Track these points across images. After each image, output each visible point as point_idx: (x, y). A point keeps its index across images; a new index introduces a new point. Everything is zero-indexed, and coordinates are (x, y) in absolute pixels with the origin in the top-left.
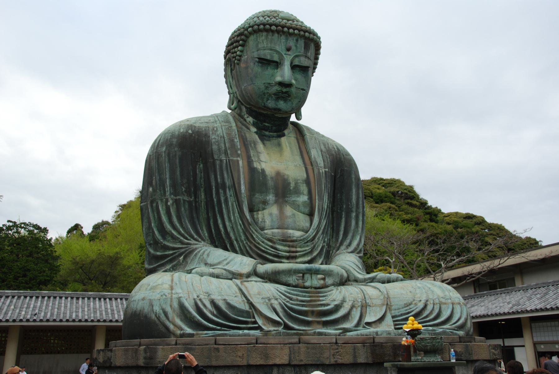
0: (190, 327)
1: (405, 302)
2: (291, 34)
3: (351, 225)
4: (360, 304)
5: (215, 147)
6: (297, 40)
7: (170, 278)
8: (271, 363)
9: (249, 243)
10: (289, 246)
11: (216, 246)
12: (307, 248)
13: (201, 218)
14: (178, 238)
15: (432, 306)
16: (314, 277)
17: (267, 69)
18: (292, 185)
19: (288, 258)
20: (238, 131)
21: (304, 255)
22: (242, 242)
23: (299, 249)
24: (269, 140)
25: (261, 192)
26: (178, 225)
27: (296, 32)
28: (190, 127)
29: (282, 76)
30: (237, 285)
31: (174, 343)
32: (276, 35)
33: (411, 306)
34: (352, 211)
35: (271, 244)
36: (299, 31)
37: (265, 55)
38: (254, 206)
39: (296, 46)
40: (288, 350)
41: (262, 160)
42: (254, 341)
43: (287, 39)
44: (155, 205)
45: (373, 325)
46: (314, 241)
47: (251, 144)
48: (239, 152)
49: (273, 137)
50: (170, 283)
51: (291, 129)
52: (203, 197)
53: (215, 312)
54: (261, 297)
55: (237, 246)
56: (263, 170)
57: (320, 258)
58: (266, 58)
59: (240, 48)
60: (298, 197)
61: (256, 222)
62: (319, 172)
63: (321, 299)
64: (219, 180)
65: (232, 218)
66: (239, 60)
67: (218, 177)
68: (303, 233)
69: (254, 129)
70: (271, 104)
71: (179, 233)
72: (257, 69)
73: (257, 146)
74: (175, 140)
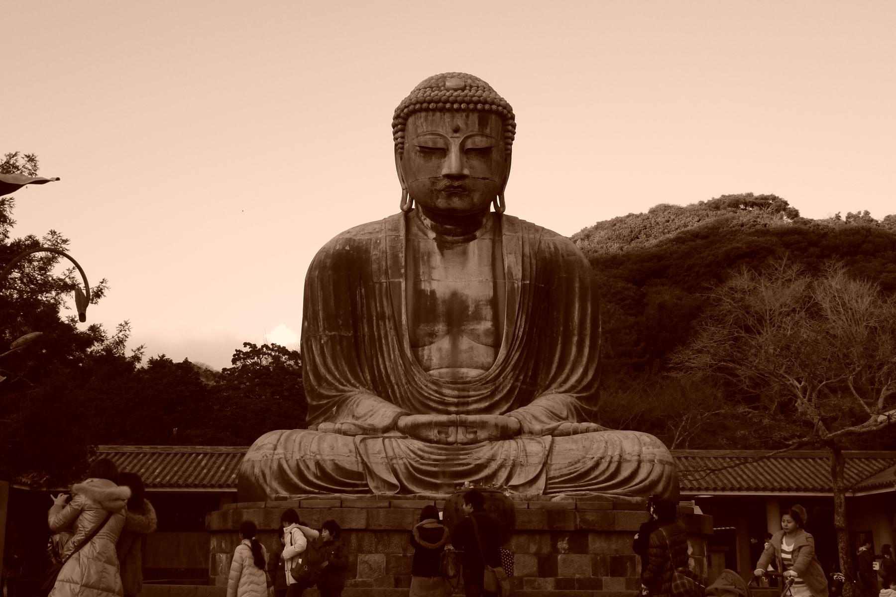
0: (287, 490)
2: (459, 110)
4: (510, 463)
5: (375, 266)
6: (467, 116)
7: (277, 437)
10: (459, 390)
13: (363, 357)
14: (332, 384)
15: (606, 464)
16: (460, 430)
17: (431, 159)
22: (403, 386)
26: (333, 368)
28: (349, 241)
29: (449, 167)
30: (355, 443)
31: (263, 506)
32: (438, 114)
33: (576, 466)
34: (574, 335)
35: (435, 388)
37: (426, 142)
39: (467, 124)
42: (338, 505)
43: (453, 117)
45: (521, 489)
47: (423, 257)
49: (458, 242)
50: (275, 442)
51: (489, 227)
52: (366, 330)
55: (397, 391)
56: (433, 292)
60: (479, 323)
61: (418, 359)
62: (513, 288)
63: (461, 457)
66: (402, 148)
68: (482, 371)
69: (432, 235)
70: (441, 203)
73: (432, 259)
74: (329, 261)
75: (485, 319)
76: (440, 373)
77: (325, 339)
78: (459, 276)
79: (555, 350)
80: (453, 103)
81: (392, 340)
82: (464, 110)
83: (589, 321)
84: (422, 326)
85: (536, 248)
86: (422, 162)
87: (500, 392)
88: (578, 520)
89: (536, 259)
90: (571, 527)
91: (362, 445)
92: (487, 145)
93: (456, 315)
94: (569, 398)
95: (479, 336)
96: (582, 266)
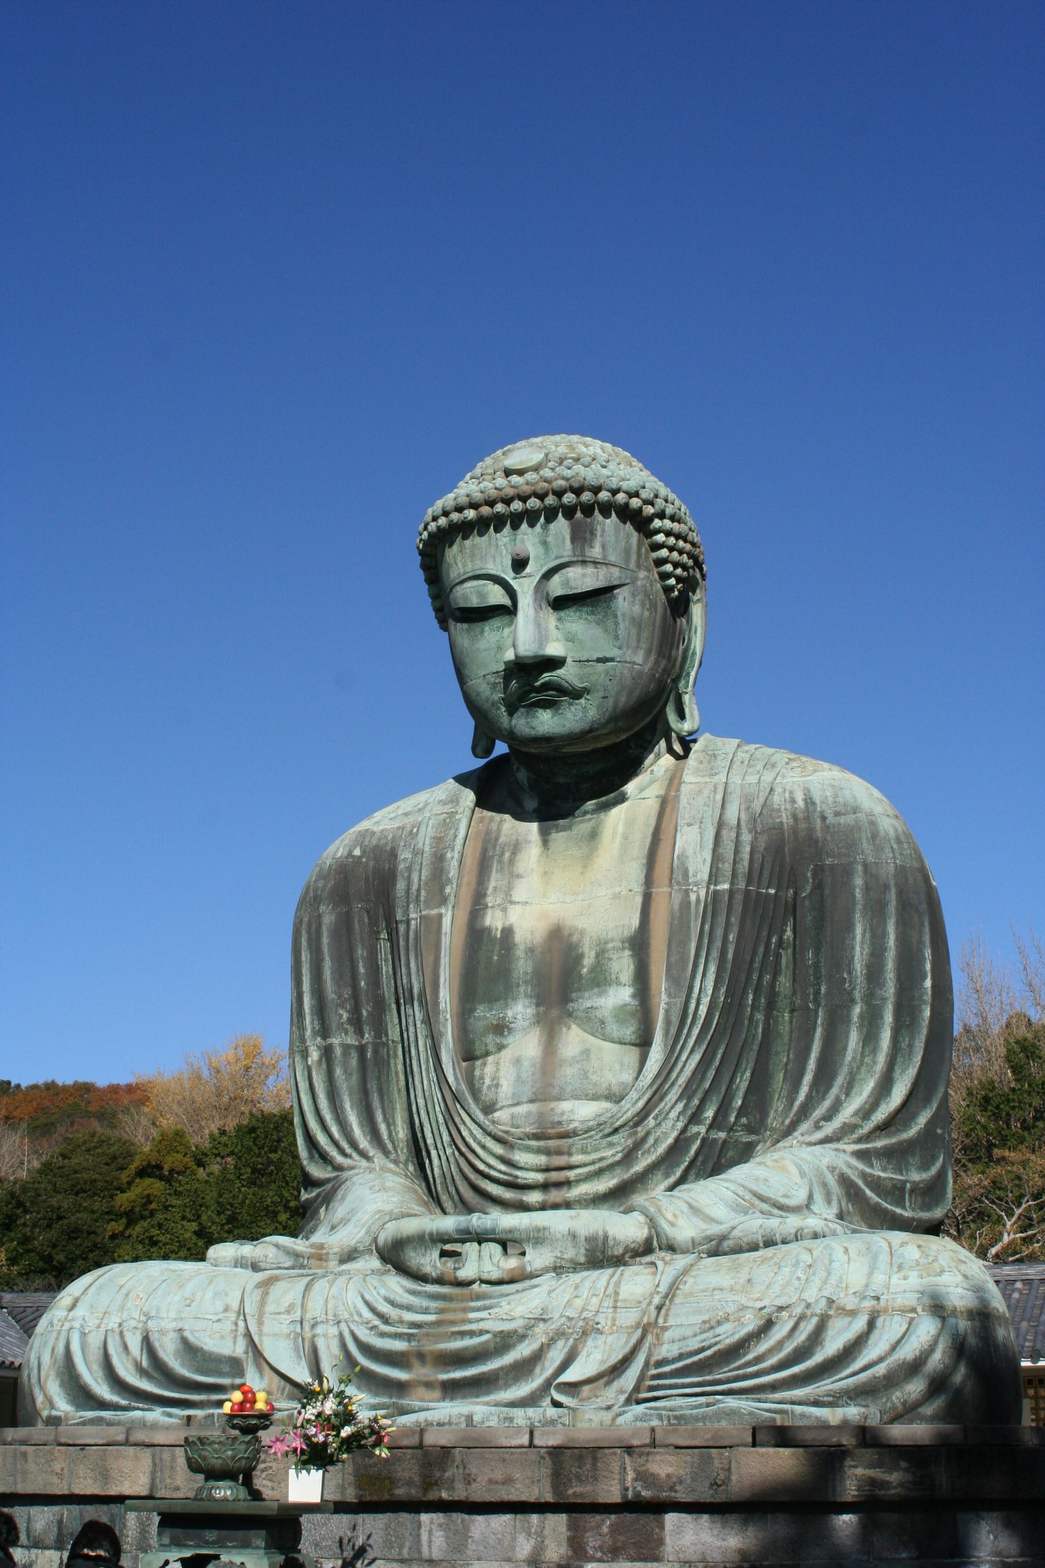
1: (706, 1317)
3: (845, 1048)
5: (401, 885)
8: (113, 1491)
9: (456, 1153)
10: (548, 1152)
12: (609, 1153)
17: (482, 632)
18: (588, 961)
19: (545, 1187)
21: (599, 1173)
23: (577, 1158)
24: (569, 828)
25: (491, 999)
26: (328, 1117)
33: (719, 1330)
34: (853, 1001)
35: (499, 1149)
36: (541, 497)
38: (473, 1043)
39: (545, 544)
40: (150, 1462)
41: (516, 898)
46: (639, 1129)
47: (502, 854)
48: (448, 890)
53: (145, 1364)
54: (291, 1318)
56: (508, 932)
57: (667, 1176)
58: (469, 605)
62: (685, 904)
63: (472, 1315)
68: (605, 1105)
76: (513, 1117)
77: (314, 1055)
79: (812, 1041)
83: (890, 964)
84: (480, 1011)
85: (757, 805)
87: (649, 1151)
88: (630, 1475)
89: (752, 830)
90: (611, 1492)
91: (259, 1291)
92: (600, 584)
93: (562, 978)
94: (841, 1158)
95: (603, 1022)
96: (874, 836)
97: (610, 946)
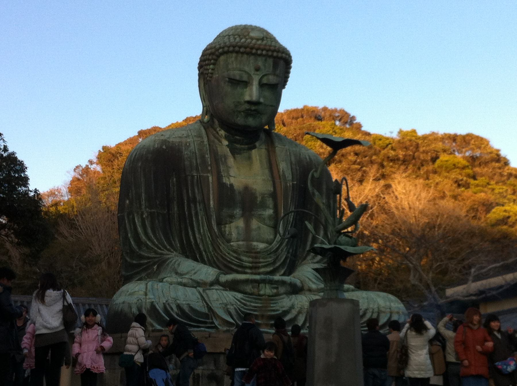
2: (260, 55)
5: (187, 163)
6: (266, 60)
10: (252, 257)
11: (187, 257)
18: (259, 199)
20: (209, 145)
23: (261, 260)
24: (240, 154)
27: (264, 52)
28: (164, 142)
29: (251, 96)
32: (245, 56)
39: (265, 66)
41: (231, 174)
44: (131, 217)
47: (221, 159)
48: (209, 168)
49: (244, 150)
52: (176, 209)
56: (232, 185)
57: (283, 268)
59: (211, 66)
61: (222, 234)
64: (190, 195)
65: (202, 231)
66: (211, 77)
67: (190, 191)
69: (226, 143)
70: (240, 120)
71: (153, 243)
72: (228, 88)
75: (269, 208)
78: (247, 174)
80: (257, 50)
81: (202, 218)
82: (264, 56)
86: (229, 90)
97: (266, 196)
